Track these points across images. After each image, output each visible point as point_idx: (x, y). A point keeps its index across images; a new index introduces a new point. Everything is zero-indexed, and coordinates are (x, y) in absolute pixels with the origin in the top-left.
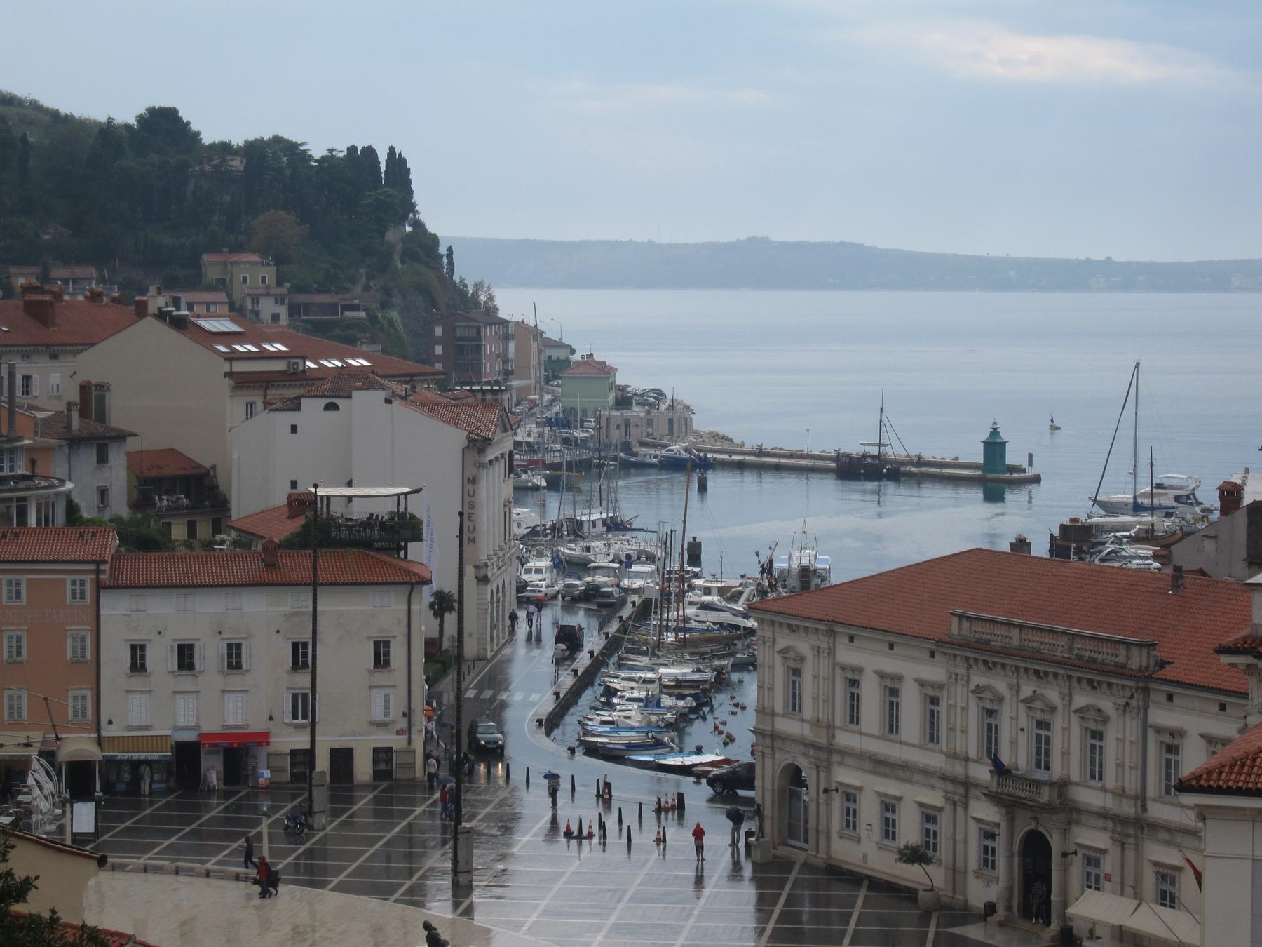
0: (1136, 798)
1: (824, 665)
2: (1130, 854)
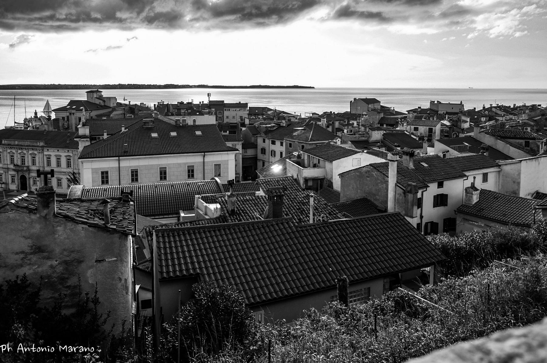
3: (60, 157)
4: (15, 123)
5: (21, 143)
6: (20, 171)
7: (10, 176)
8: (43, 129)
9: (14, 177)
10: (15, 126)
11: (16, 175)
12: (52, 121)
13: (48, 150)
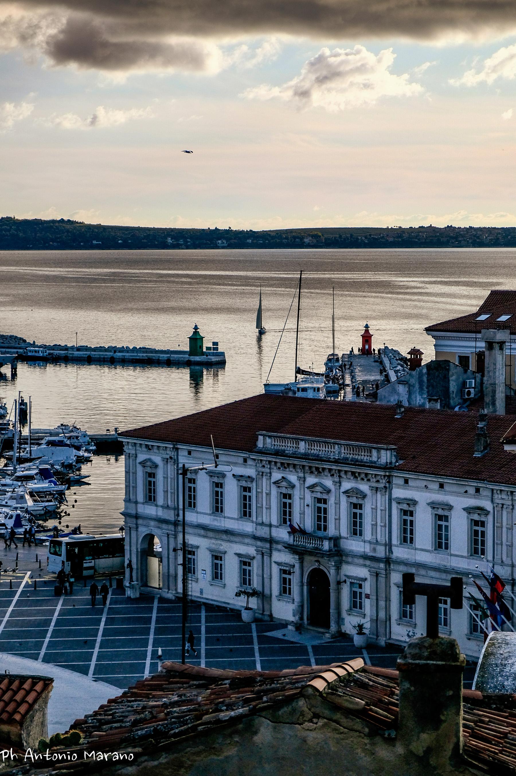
0: (385, 545)
1: (171, 468)
2: (382, 580)
3: (446, 513)
4: (299, 371)
5: (317, 450)
6: (311, 553)
7: (275, 570)
8: (393, 400)
9: (290, 573)
10: (296, 383)
11: (297, 566)
12: (425, 371)
13: (406, 481)
